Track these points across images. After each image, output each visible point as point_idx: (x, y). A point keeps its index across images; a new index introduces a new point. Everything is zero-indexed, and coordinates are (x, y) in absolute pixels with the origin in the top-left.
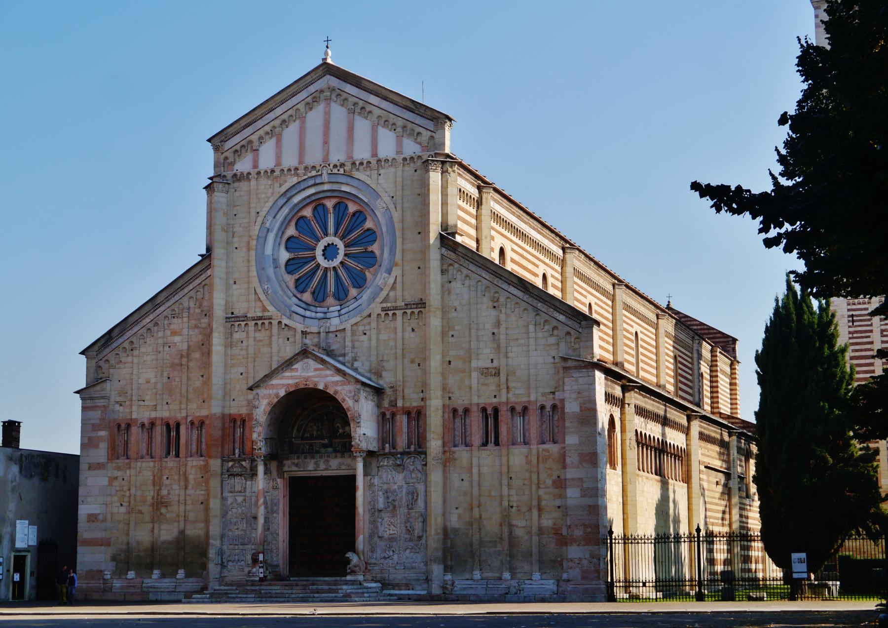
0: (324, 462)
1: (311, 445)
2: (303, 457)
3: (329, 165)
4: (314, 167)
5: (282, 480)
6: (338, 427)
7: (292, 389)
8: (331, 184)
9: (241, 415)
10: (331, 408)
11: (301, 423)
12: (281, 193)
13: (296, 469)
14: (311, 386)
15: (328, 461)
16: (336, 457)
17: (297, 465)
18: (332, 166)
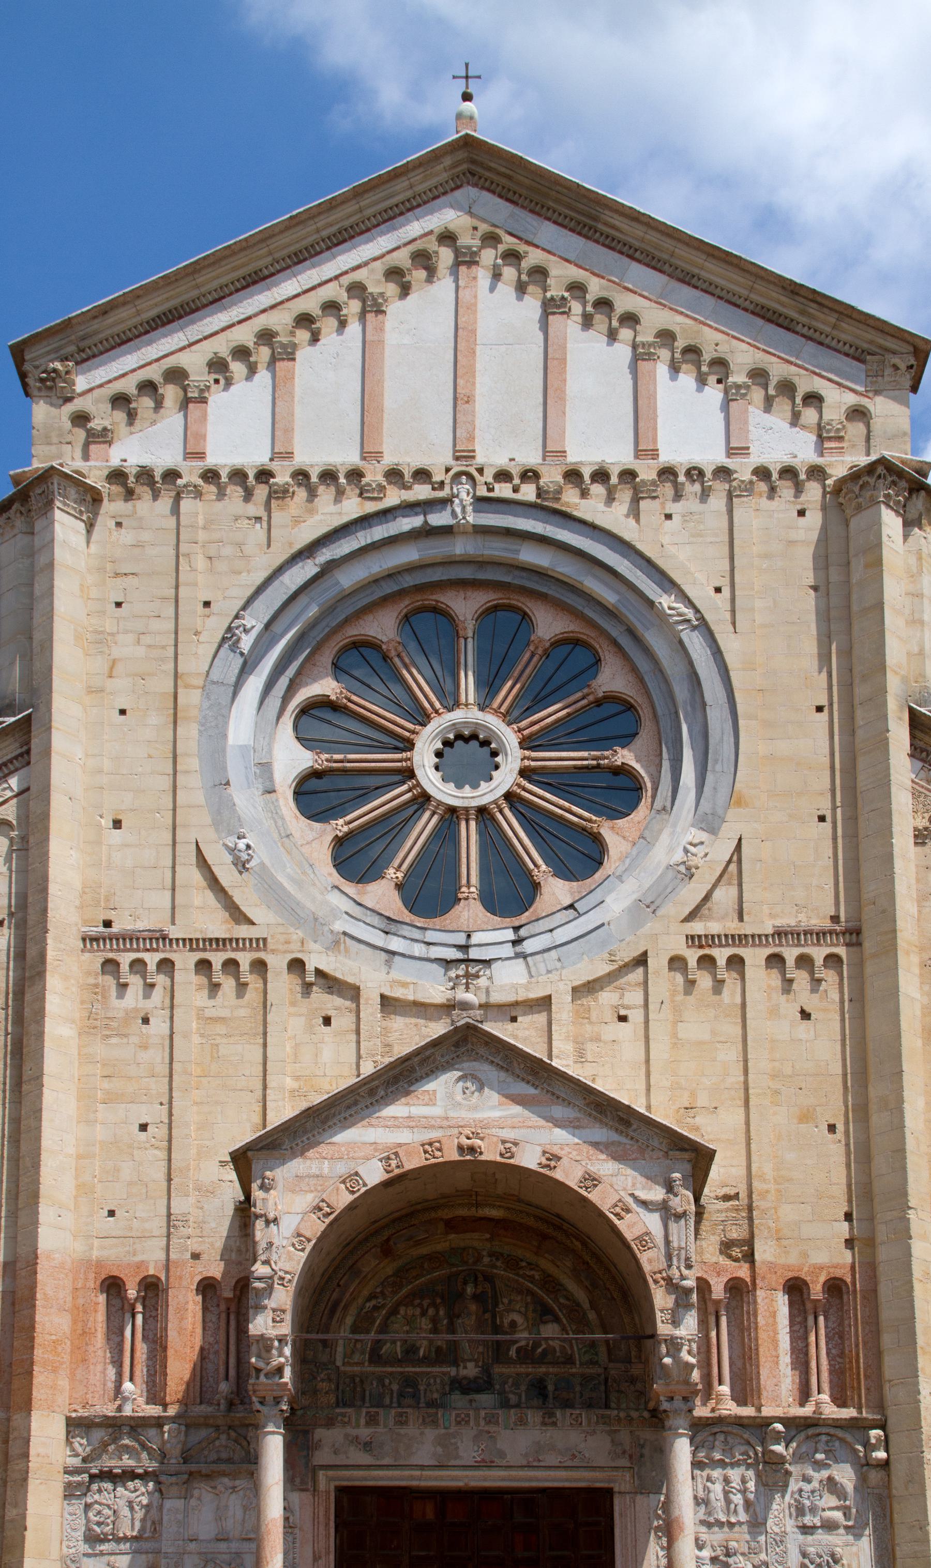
0: (476, 1439)
1: (409, 1382)
2: (391, 1422)
3: (481, 471)
4: (422, 475)
5: (307, 1497)
6: (513, 1324)
7: (413, 1162)
8: (480, 539)
9: (140, 1265)
10: (486, 1260)
11: (369, 1305)
12: (298, 546)
13: (366, 1459)
14: (490, 1154)
15: (493, 1438)
16: (522, 1422)
17: (367, 1446)
18: (488, 477)
